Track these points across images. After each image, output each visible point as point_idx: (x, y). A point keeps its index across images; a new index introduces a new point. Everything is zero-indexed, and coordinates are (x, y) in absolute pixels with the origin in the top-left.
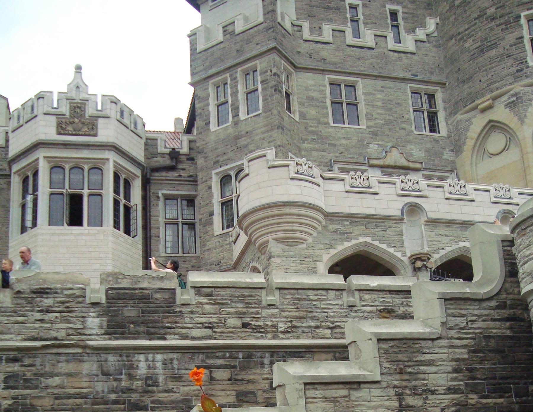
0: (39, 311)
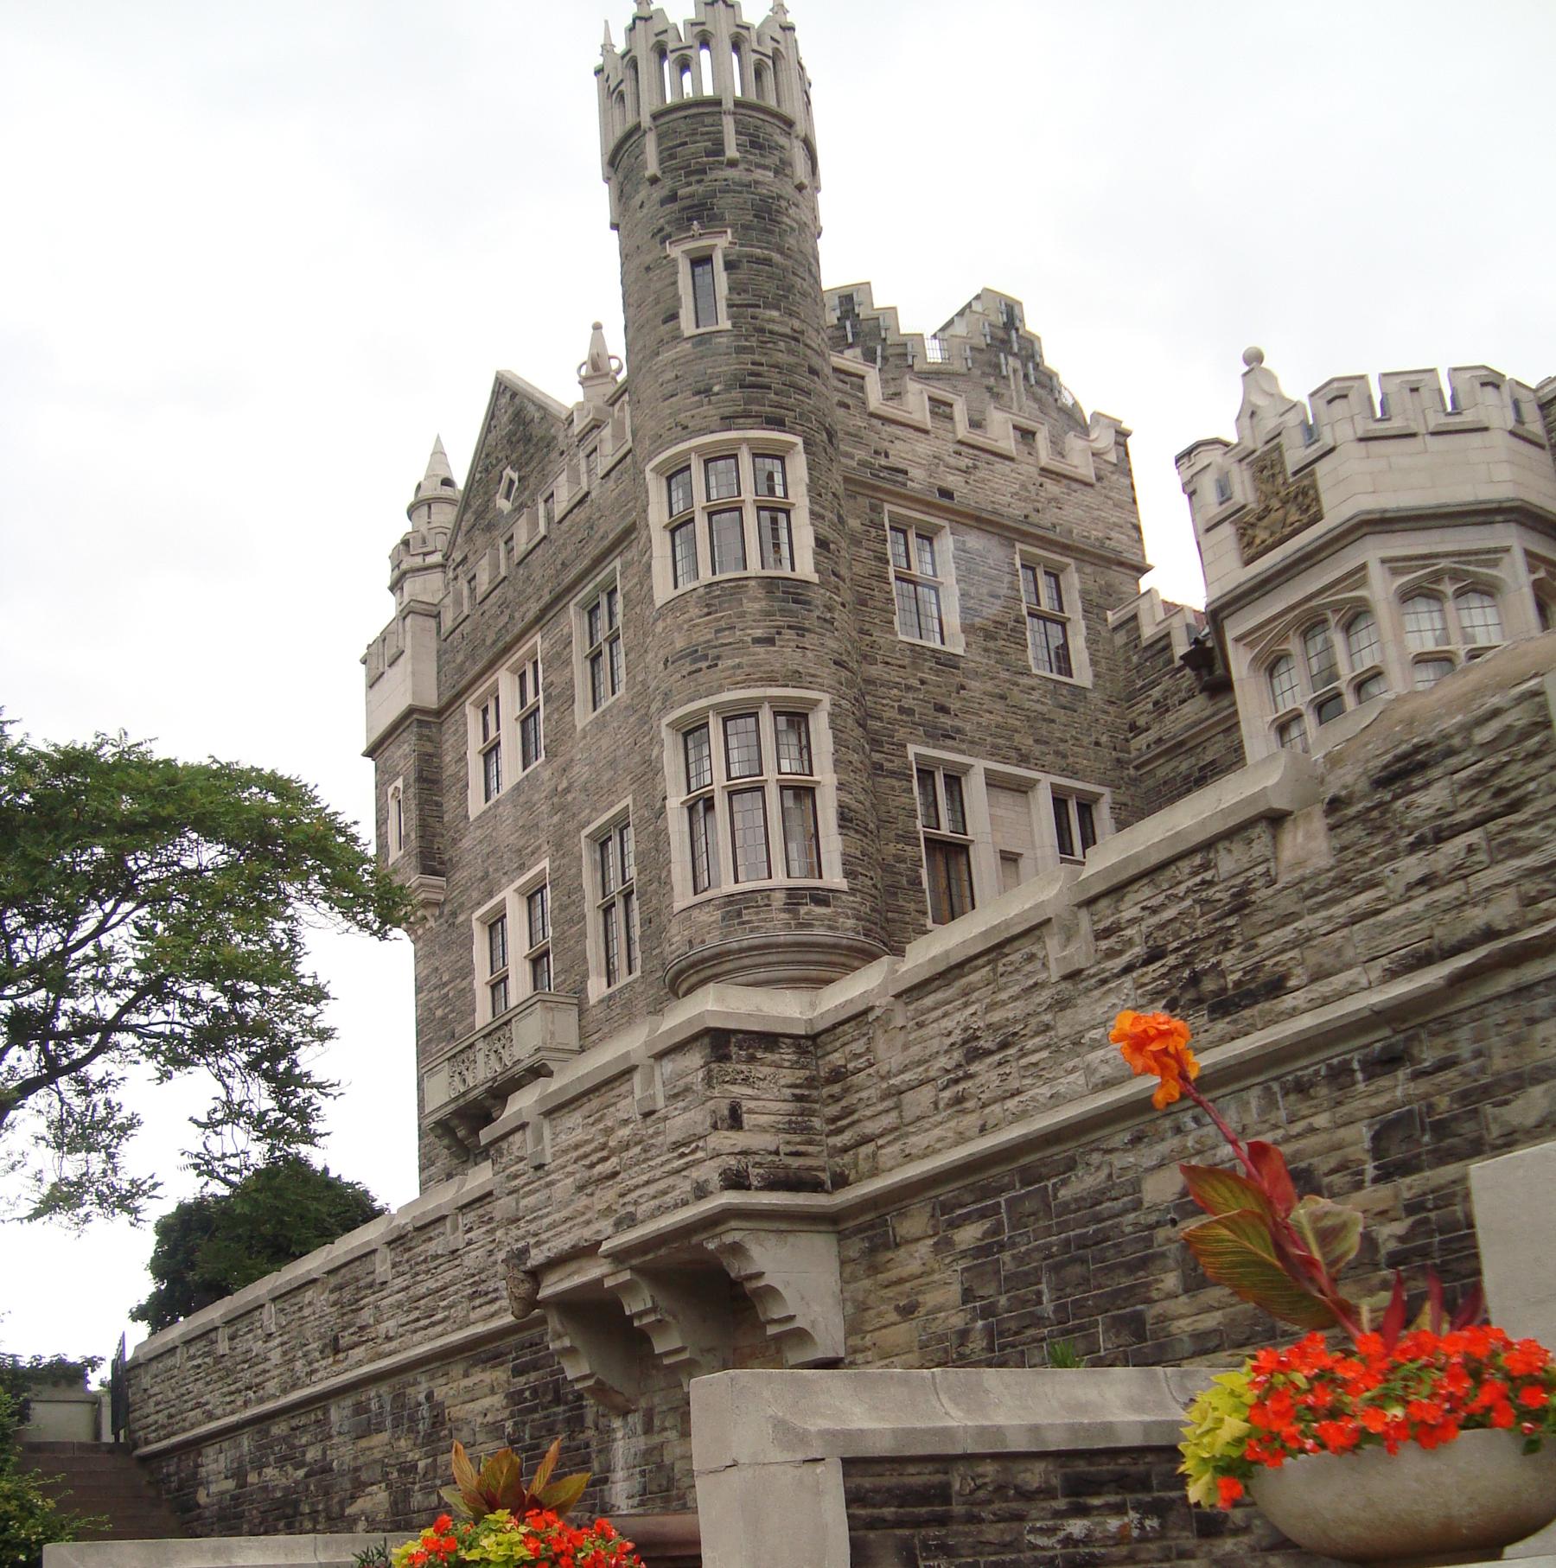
0: (1413, 848)
